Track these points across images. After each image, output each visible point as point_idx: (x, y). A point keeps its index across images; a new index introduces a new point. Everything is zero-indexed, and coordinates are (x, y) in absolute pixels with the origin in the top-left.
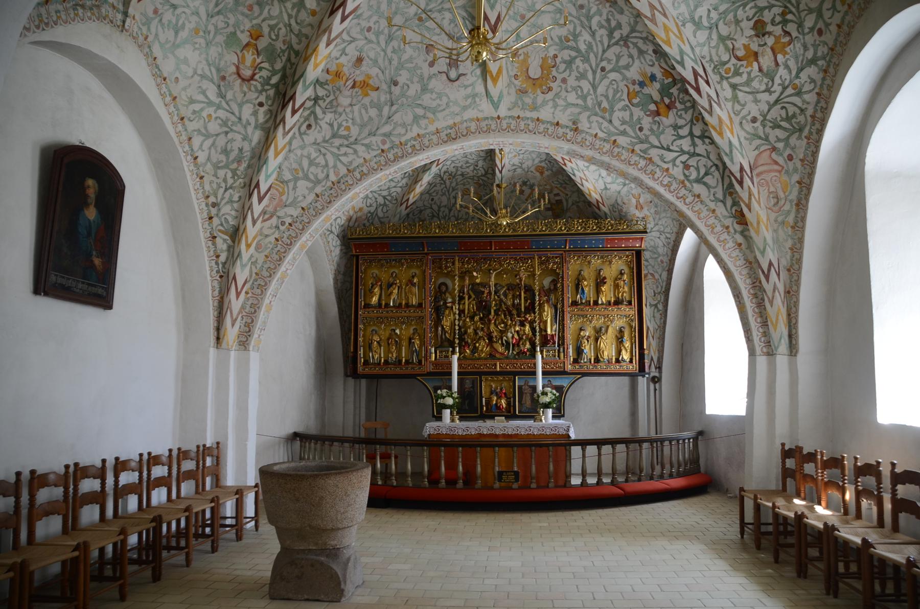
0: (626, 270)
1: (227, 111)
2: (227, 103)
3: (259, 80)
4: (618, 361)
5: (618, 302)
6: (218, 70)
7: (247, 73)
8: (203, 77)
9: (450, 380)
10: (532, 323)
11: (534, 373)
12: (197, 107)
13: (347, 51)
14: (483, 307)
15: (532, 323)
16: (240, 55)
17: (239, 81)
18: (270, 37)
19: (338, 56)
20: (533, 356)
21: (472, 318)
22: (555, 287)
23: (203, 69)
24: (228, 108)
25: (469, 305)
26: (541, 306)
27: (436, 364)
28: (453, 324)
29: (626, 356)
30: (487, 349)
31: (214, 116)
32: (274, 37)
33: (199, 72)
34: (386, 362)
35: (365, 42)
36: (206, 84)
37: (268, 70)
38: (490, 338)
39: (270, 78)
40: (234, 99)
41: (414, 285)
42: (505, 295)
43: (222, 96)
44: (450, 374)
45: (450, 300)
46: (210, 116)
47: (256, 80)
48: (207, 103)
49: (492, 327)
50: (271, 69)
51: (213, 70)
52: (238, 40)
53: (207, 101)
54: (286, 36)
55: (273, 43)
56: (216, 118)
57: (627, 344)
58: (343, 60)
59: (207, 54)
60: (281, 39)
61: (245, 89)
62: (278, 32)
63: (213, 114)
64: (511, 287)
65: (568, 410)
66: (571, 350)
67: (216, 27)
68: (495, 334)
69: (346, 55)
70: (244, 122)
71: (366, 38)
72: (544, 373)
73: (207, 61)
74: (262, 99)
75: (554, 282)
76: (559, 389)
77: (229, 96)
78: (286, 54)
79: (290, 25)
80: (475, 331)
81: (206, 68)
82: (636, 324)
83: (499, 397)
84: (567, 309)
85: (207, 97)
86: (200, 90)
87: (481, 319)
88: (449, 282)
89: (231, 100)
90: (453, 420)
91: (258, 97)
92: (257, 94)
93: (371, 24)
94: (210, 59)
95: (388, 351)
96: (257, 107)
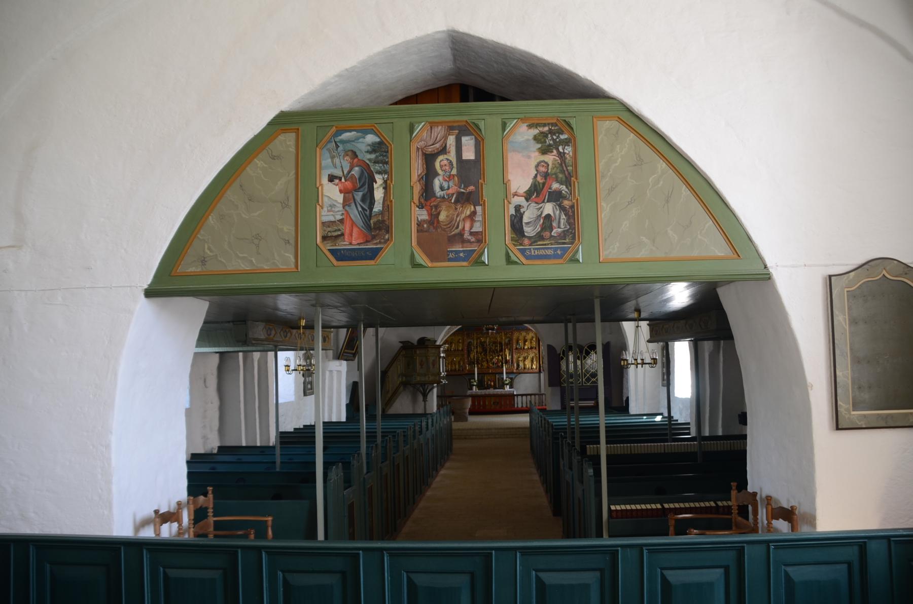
0: (534, 336)
4: (532, 368)
5: (532, 348)
9: (474, 376)
10: (502, 356)
11: (503, 373)
14: (484, 350)
15: (502, 356)
20: (502, 367)
21: (481, 354)
22: (509, 343)
25: (479, 349)
26: (505, 350)
27: (469, 371)
28: (474, 356)
29: (534, 367)
30: (486, 365)
34: (451, 370)
38: (487, 361)
41: (460, 342)
42: (492, 346)
44: (474, 374)
45: (473, 348)
49: (488, 357)
57: (535, 363)
64: (495, 343)
65: (514, 385)
66: (515, 365)
68: (489, 360)
72: (506, 373)
75: (509, 341)
76: (511, 379)
80: (482, 359)
82: (538, 355)
83: (491, 382)
84: (514, 351)
87: (484, 355)
88: (472, 342)
90: (476, 390)
95: (452, 367)
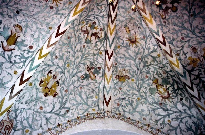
1: (173, 113)
2: (171, 111)
3: (172, 92)
6: (157, 103)
7: (166, 94)
8: (154, 110)
12: (161, 122)
13: (185, 52)
16: (158, 92)
17: (167, 100)
18: (160, 77)
19: (185, 56)
23: (151, 108)
24: (173, 112)
31: (170, 119)
32: (161, 76)
33: (151, 110)
35: (187, 43)
36: (157, 112)
37: (171, 86)
39: (174, 88)
40: (172, 107)
43: (166, 110)
46: (168, 121)
47: (171, 94)
48: (163, 117)
50: (171, 85)
51: (155, 105)
52: (153, 88)
53: (162, 116)
54: (162, 71)
55: (162, 77)
56: (172, 119)
58: (188, 55)
59: (148, 102)
60: (163, 74)
61: (171, 100)
62: (160, 73)
63: (169, 119)
67: (144, 92)
69: (187, 53)
70: (183, 111)
71: (186, 42)
73: (150, 104)
74: (180, 97)
77: (169, 107)
78: (169, 75)
79: (160, 67)
81: (152, 107)
85: (161, 115)
86: (157, 115)
89: (171, 109)
91: (178, 98)
92: (176, 98)
93: (181, 37)
94: (151, 103)
96: (181, 102)
